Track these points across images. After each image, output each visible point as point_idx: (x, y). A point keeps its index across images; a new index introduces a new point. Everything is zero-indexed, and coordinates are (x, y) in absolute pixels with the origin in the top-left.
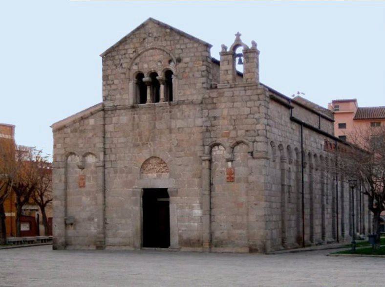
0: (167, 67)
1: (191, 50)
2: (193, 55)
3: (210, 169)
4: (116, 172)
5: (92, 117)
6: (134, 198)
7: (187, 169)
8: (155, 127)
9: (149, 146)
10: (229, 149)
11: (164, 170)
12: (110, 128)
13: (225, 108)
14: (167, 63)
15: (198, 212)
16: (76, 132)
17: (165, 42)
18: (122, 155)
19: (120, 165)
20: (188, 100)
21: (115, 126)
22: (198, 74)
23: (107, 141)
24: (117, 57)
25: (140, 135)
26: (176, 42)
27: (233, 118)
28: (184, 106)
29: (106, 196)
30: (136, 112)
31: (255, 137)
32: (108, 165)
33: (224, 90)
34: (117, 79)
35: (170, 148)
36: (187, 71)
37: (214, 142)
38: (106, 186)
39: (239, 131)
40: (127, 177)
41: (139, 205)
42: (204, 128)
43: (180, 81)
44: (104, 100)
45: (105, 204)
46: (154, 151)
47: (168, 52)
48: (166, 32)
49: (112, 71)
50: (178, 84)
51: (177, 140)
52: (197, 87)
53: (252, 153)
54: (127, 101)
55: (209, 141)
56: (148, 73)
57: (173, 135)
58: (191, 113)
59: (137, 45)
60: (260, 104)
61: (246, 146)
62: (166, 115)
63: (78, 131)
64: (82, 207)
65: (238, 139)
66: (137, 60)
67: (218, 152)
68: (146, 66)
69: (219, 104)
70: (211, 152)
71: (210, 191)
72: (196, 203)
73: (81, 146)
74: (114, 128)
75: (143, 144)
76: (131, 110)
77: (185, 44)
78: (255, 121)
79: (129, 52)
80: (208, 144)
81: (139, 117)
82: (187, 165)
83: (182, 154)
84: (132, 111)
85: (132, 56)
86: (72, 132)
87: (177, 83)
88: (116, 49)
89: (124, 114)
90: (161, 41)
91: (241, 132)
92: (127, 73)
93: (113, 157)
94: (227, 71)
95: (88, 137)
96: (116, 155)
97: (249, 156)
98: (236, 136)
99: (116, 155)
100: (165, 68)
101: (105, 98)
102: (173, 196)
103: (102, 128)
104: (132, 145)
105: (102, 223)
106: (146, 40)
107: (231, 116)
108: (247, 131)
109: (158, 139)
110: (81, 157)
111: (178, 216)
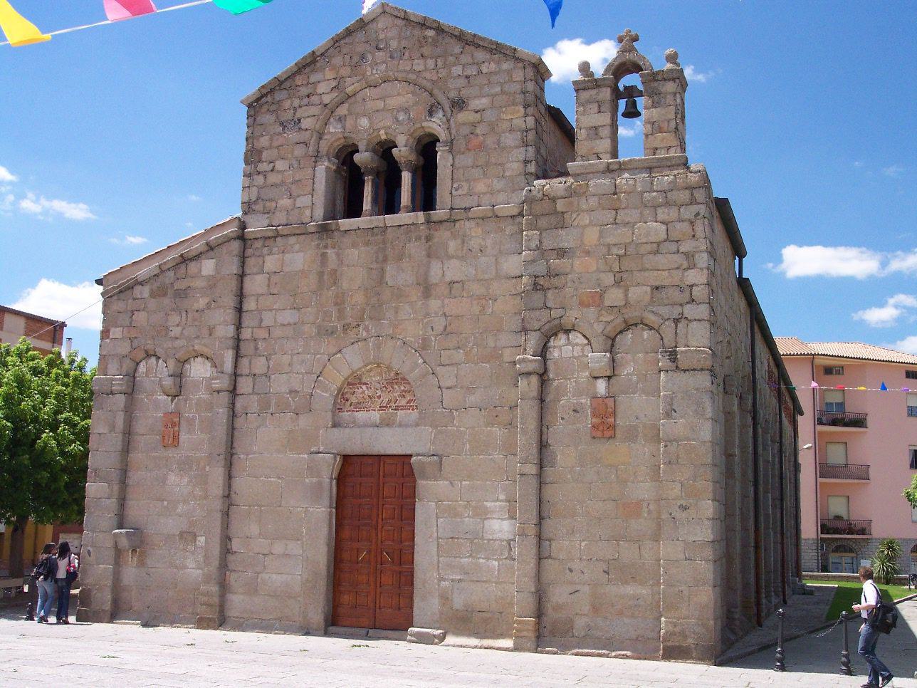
1: (494, 78)
2: (498, 89)
3: (542, 400)
5: (211, 254)
6: (315, 480)
8: (381, 280)
9: (365, 334)
10: (598, 342)
11: (403, 402)
12: (255, 284)
13: (591, 224)
14: (425, 114)
15: (501, 527)
16: (165, 295)
17: (421, 61)
18: (286, 359)
19: (279, 385)
21: (269, 279)
22: (510, 140)
23: (247, 320)
24: (287, 104)
25: (339, 302)
29: (234, 473)
30: (330, 241)
32: (245, 385)
35: (424, 340)
38: (235, 445)
39: (632, 290)
41: (326, 502)
42: (524, 279)
44: (245, 213)
45: (228, 496)
47: (428, 85)
49: (271, 140)
52: (507, 174)
53: (673, 355)
55: (539, 319)
57: (434, 304)
60: (698, 214)
62: (416, 249)
63: (170, 292)
64: (165, 503)
65: (632, 314)
66: (343, 110)
67: (567, 351)
68: (364, 122)
70: (543, 352)
71: (541, 466)
72: (498, 500)
73: (176, 331)
75: (346, 328)
78: (678, 259)
79: (320, 90)
81: (338, 255)
82: (470, 390)
83: (460, 355)
84: (319, 238)
85: (327, 99)
88: (287, 85)
89: (297, 247)
90: (411, 58)
91: (639, 293)
92: (312, 141)
93: (260, 365)
94: (596, 128)
95: (196, 306)
97: (664, 362)
98: (623, 303)
101: (248, 207)
102: (427, 479)
103: (234, 284)
105: (216, 551)
107: (609, 246)
108: (657, 288)
110: (171, 363)
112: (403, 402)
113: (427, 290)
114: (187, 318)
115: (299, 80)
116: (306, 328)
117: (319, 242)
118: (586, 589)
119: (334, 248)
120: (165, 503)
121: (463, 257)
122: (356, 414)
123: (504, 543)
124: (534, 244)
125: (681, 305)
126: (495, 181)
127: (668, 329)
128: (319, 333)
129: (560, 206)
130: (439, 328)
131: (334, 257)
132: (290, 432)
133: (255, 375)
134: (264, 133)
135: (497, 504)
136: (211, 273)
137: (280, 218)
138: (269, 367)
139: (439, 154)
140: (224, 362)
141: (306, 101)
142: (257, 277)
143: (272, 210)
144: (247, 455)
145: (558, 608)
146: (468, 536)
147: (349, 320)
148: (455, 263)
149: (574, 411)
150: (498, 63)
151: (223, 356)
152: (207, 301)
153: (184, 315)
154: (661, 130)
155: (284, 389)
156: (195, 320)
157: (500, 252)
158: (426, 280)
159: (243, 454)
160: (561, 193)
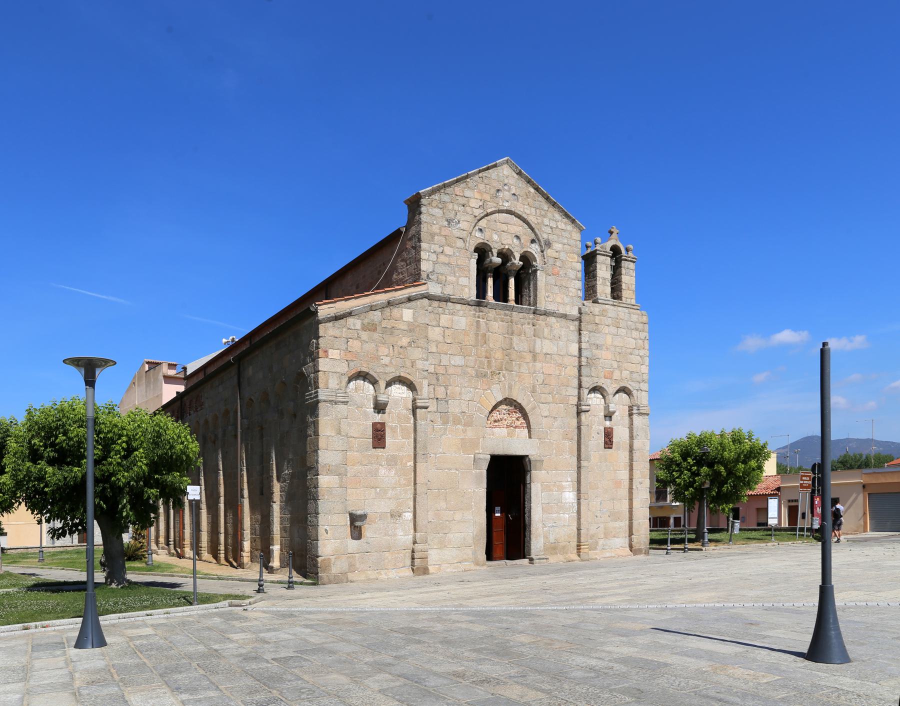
0: (529, 250)
4: (446, 422)
7: (556, 424)
8: (511, 347)
9: (503, 379)
16: (375, 330)
20: (558, 311)
21: (444, 331)
22: (572, 274)
24: (450, 206)
27: (618, 350)
28: (552, 320)
30: (481, 314)
31: (640, 383)
33: (607, 306)
34: (452, 247)
36: (558, 263)
37: (595, 385)
39: (624, 372)
40: (464, 431)
43: (548, 277)
46: (510, 388)
47: (533, 225)
48: (529, 192)
49: (440, 229)
51: (543, 373)
54: (467, 290)
57: (538, 365)
58: (563, 333)
59: (487, 197)
61: (626, 395)
62: (528, 329)
63: (379, 328)
64: (378, 490)
66: (483, 223)
68: (495, 237)
72: (568, 481)
73: (386, 360)
75: (493, 373)
77: (556, 221)
80: (587, 387)
81: (487, 324)
83: (550, 398)
86: (365, 328)
89: (461, 313)
95: (400, 343)
96: (446, 387)
99: (446, 387)
100: (525, 250)
104: (473, 373)
106: (501, 194)
109: (516, 368)
111: (542, 504)
112: (518, 423)
113: (535, 358)
116: (469, 370)
118: (602, 525)
120: (378, 490)
121: (551, 339)
122: (494, 429)
123: (571, 505)
125: (640, 383)
126: (565, 298)
127: (634, 392)
128: (477, 375)
129: (597, 320)
130: (540, 381)
132: (462, 439)
133: (437, 399)
134: (435, 222)
135: (568, 483)
136: (412, 321)
137: (449, 291)
138: (447, 394)
139: (538, 272)
140: (423, 387)
142: (435, 328)
143: (443, 282)
144: (436, 454)
145: (592, 537)
146: (555, 502)
147: (493, 369)
148: (547, 341)
149: (598, 433)
150: (565, 224)
151: (421, 383)
152: (409, 341)
155: (457, 410)
156: (400, 354)
157: (568, 340)
158: (534, 350)
159: (433, 454)
160: (597, 313)
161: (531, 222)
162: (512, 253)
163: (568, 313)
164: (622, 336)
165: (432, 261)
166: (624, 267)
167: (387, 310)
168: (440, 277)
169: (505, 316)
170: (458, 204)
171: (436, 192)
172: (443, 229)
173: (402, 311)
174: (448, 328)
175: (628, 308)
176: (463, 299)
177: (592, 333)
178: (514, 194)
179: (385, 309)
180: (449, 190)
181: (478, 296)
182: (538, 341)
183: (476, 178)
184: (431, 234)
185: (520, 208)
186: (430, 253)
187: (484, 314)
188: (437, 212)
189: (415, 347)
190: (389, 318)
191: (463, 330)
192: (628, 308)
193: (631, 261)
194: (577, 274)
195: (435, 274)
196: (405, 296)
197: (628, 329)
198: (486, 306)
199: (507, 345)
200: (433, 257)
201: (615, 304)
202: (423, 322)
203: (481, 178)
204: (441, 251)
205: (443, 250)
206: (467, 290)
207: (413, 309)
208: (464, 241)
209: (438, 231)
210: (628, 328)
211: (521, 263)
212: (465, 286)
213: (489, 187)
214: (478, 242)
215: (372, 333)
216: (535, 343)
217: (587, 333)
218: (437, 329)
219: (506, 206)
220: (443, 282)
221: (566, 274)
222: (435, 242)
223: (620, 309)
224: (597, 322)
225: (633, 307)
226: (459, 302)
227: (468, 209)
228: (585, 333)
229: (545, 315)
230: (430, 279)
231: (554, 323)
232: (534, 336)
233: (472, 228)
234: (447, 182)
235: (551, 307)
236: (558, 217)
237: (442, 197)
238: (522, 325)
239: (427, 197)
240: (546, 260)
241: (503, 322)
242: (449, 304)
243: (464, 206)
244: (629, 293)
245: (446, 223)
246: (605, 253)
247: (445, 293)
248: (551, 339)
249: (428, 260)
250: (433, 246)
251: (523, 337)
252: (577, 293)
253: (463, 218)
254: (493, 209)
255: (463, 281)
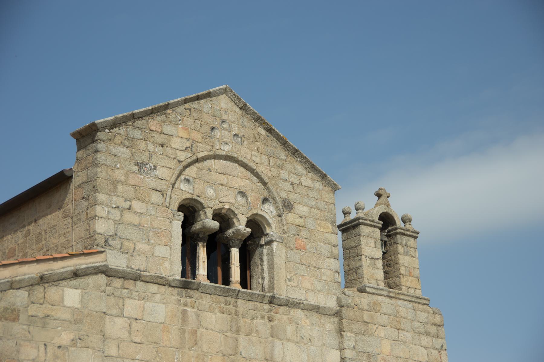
0: (260, 212)
14: (259, 203)
16: (16, 319)
20: (307, 300)
21: (130, 325)
22: (325, 249)
26: (279, 162)
28: (298, 313)
30: (189, 300)
33: (379, 297)
34: (144, 202)
36: (304, 233)
47: (265, 178)
48: (259, 134)
49: (126, 175)
50: (286, 258)
54: (167, 264)
56: (215, 210)
58: (315, 333)
59: (198, 137)
62: (262, 325)
63: (23, 317)
66: (191, 172)
68: (210, 192)
69: (375, 327)
74: (130, 333)
76: (177, 290)
81: (198, 316)
85: (182, 156)
87: (284, 255)
89: (158, 297)
92: (169, 192)
95: (57, 341)
100: (254, 212)
106: (217, 133)
114: (46, 353)
115: (153, 123)
117: (179, 298)
119: (193, 308)
121: (297, 342)
124: (352, 344)
126: (316, 282)
129: (366, 316)
131: (193, 314)
134: (118, 165)
136: (79, 306)
137: (138, 264)
141: (158, 149)
143: (131, 251)
148: (291, 345)
150: (312, 179)
153: (42, 348)
154: (410, 275)
157: (324, 344)
161: (261, 174)
162: (235, 215)
163: (321, 305)
164: (405, 342)
165: (113, 220)
166: (402, 244)
167: (39, 291)
168: (125, 243)
169: (226, 304)
170: (154, 143)
171: (120, 124)
172: (131, 176)
173: (63, 291)
174: (136, 319)
175: (412, 301)
176: (162, 278)
177: (360, 336)
178: (236, 135)
179: (36, 287)
180: (140, 123)
181: (184, 274)
182: (277, 343)
183: (181, 109)
184: (112, 182)
185: (245, 155)
186: (110, 209)
187: (193, 300)
188: (123, 152)
189: (81, 347)
190: (41, 301)
191: (161, 323)
192: (412, 301)
193: (410, 236)
194: (332, 249)
195: (118, 240)
196: (69, 269)
197: (414, 332)
198: (197, 289)
199: (230, 348)
200: (116, 214)
201: (391, 294)
202: (97, 309)
203: (188, 111)
204: (128, 207)
205: (131, 206)
206: (167, 264)
207: (81, 289)
208: (163, 195)
209: (123, 178)
210: (414, 331)
211: (249, 230)
212: (164, 258)
213: (199, 123)
214: (184, 197)
215: (11, 323)
216: (273, 346)
217: (352, 335)
218: (120, 322)
219: (226, 149)
220: (131, 251)
221: (316, 249)
222: (119, 194)
223: (399, 302)
224: (366, 319)
225: (419, 301)
226: (156, 281)
227: (169, 151)
228: (349, 334)
229: (286, 305)
230: (109, 246)
231: (301, 318)
232: (272, 336)
233: (174, 177)
234: (137, 111)
235: (296, 295)
236: (300, 170)
237: (130, 132)
238: (253, 319)
239: (107, 131)
240: (285, 228)
241: (223, 313)
242: (139, 283)
243: (162, 146)
244: (412, 281)
245: (136, 168)
246: (372, 223)
247: (133, 267)
248: (297, 342)
249: (107, 218)
250: (115, 199)
251: (254, 336)
252: (334, 276)
253: (161, 163)
254: (206, 153)
255: (161, 251)
